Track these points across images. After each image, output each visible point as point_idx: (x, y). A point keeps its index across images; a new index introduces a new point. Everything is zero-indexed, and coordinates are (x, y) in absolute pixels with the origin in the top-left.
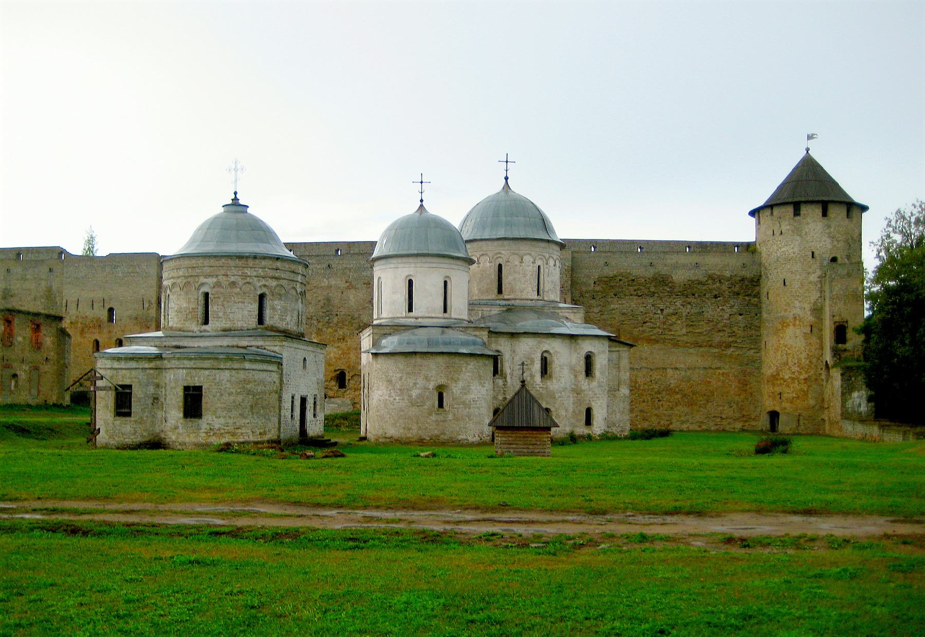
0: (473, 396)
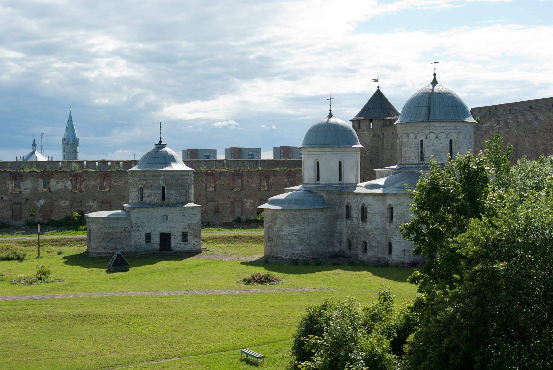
0: (284, 233)
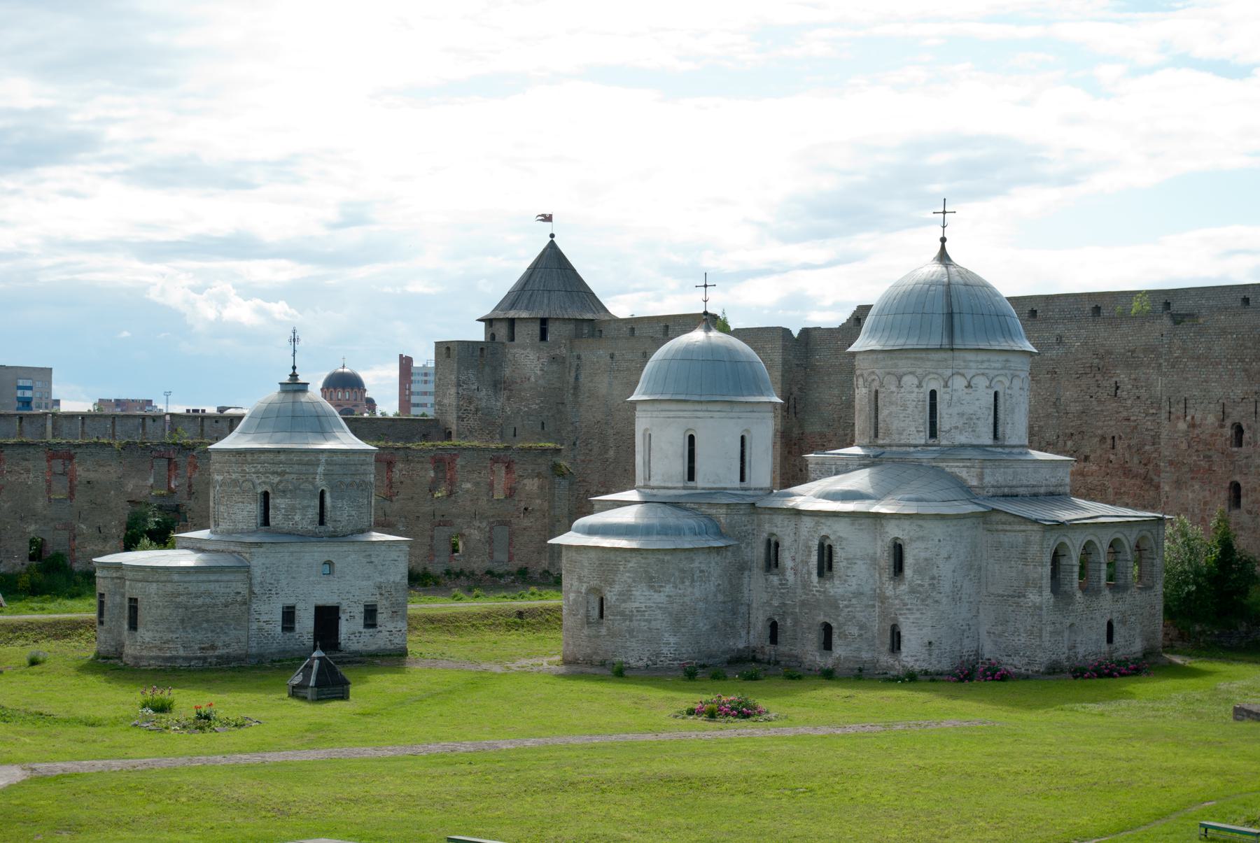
0: (637, 605)
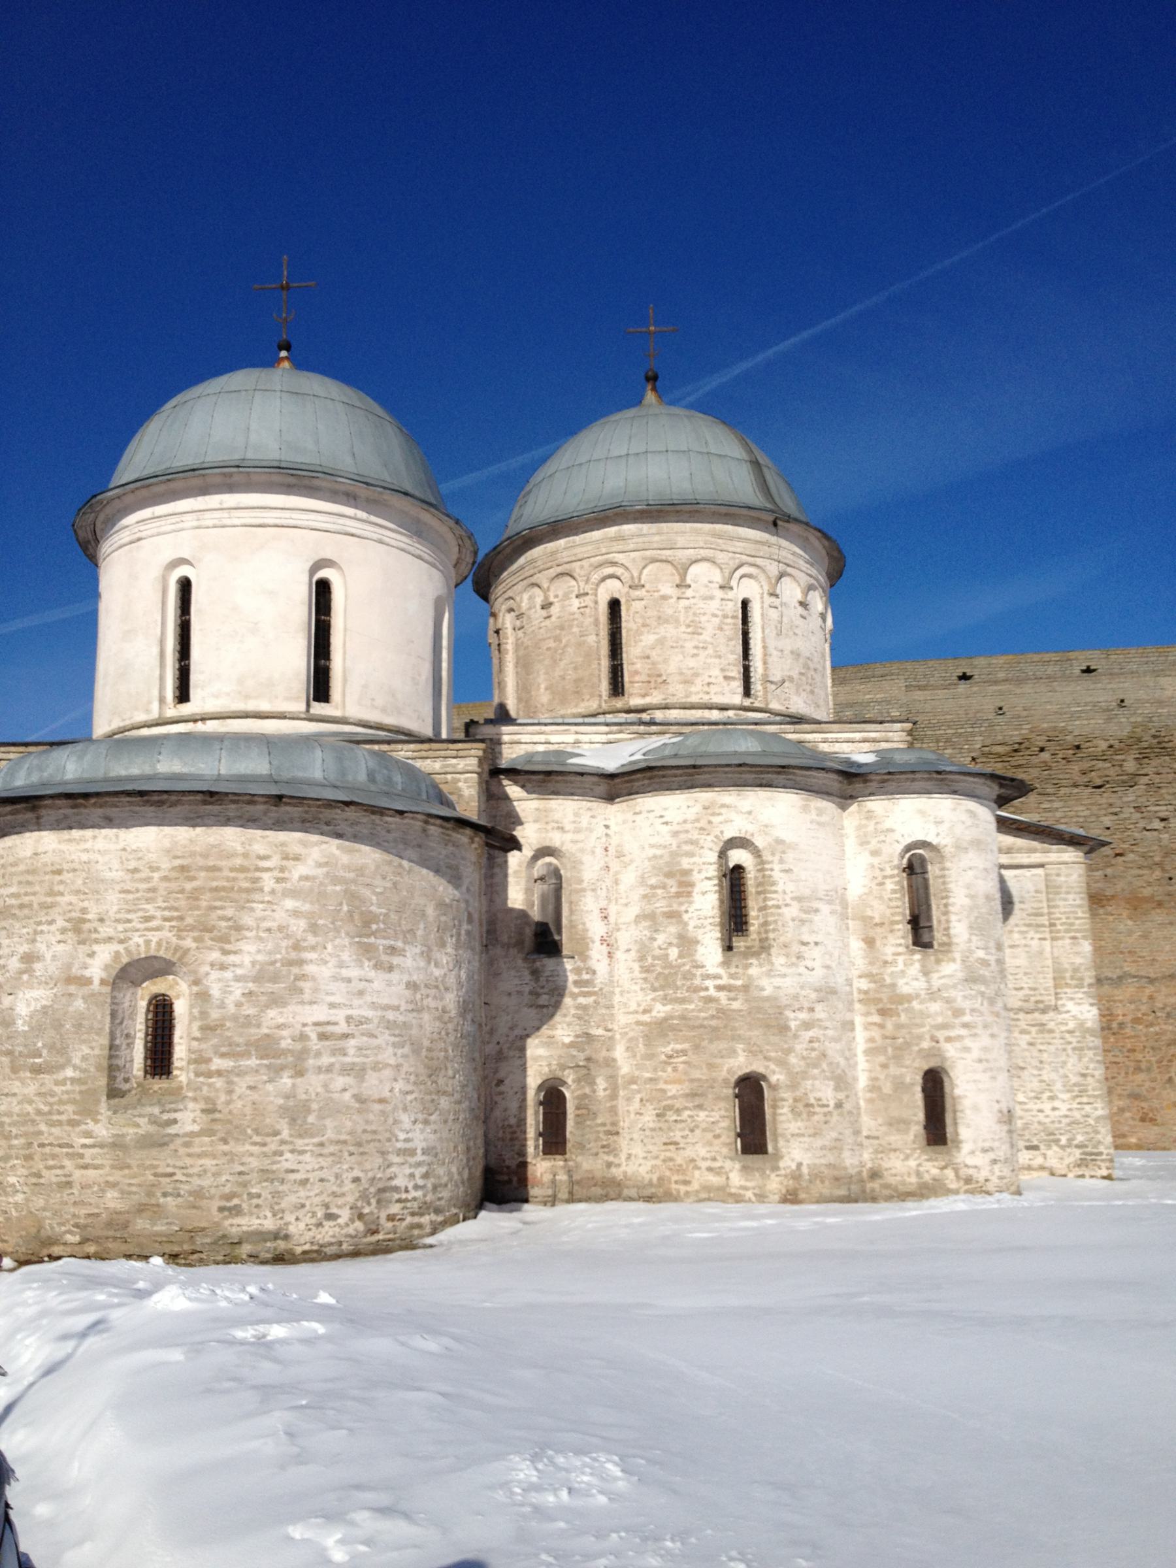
0: (320, 1013)
